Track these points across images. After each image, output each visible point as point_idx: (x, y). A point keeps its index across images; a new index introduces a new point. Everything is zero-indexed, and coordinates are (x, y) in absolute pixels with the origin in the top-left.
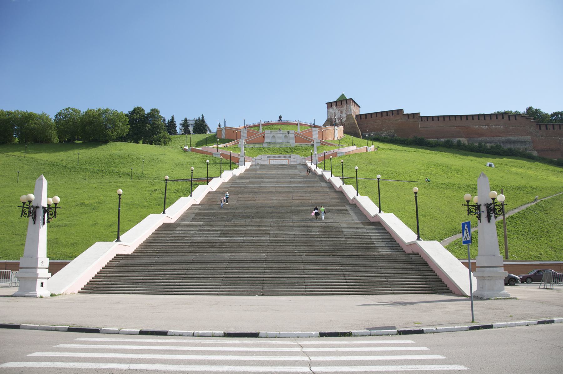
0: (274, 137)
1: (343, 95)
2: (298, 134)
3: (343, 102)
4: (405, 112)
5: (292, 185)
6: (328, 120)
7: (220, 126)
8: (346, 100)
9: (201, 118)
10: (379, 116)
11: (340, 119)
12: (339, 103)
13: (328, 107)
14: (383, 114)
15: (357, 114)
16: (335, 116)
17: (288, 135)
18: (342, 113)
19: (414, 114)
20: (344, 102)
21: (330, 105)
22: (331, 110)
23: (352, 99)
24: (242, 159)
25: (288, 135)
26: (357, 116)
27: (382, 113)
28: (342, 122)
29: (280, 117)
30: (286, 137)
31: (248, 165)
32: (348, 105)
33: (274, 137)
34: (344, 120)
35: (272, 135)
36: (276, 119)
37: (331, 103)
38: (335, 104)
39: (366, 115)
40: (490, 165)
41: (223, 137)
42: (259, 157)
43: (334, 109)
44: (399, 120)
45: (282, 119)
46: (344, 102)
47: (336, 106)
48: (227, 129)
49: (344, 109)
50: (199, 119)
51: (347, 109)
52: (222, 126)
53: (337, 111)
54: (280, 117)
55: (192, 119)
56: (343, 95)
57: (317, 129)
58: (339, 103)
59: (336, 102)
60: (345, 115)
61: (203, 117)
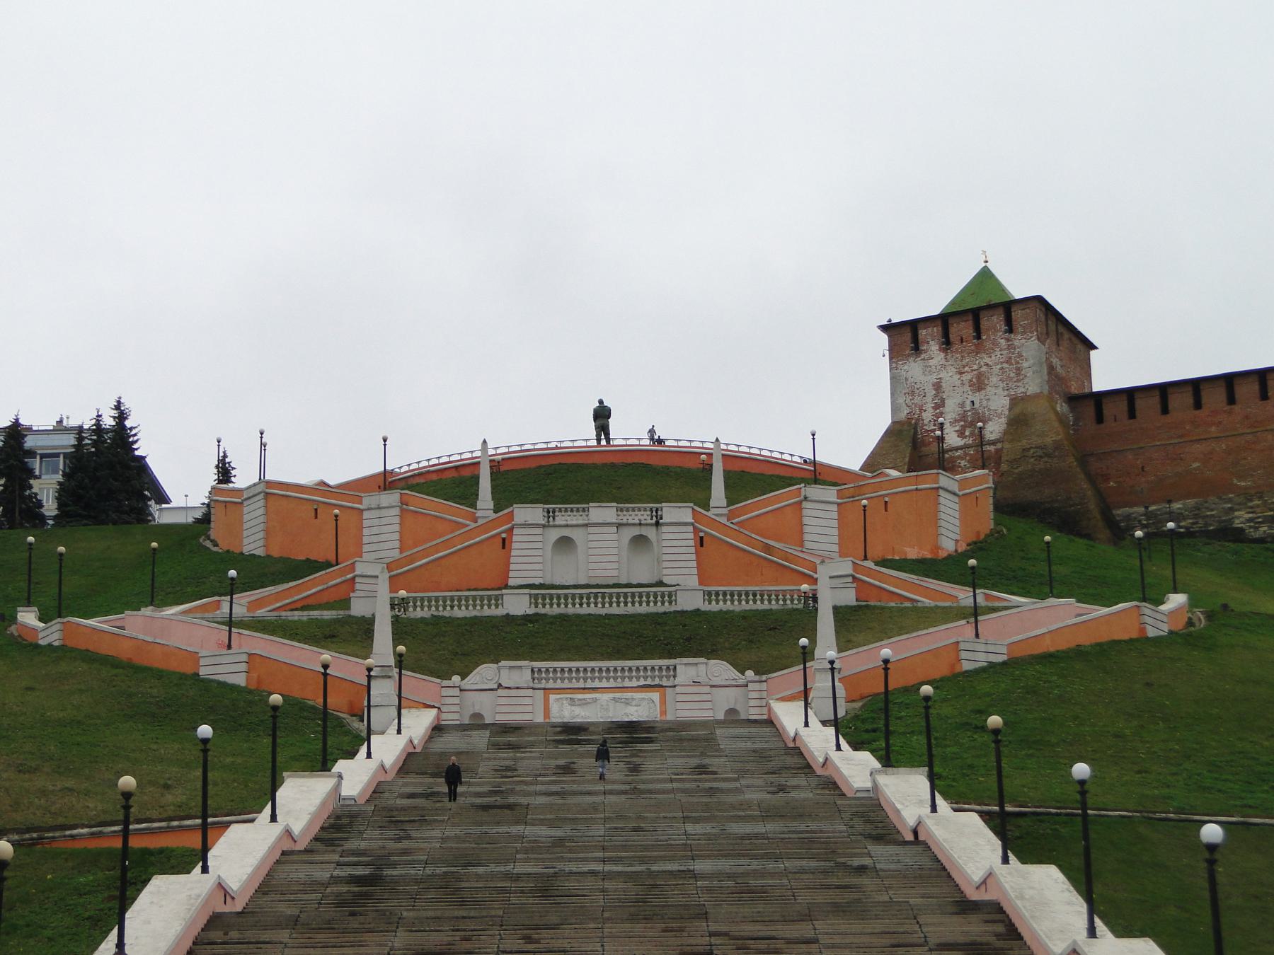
0: (565, 543)
1: (985, 276)
2: (713, 523)
3: (982, 315)
5: (699, 866)
6: (893, 434)
7: (224, 472)
8: (1008, 307)
9: (108, 422)
10: (1213, 399)
11: (972, 421)
12: (962, 329)
13: (895, 353)
14: (1242, 390)
15: (1074, 389)
16: (940, 405)
17: (651, 533)
18: (979, 384)
20: (995, 321)
21: (905, 336)
22: (913, 369)
23: (1039, 300)
24: (383, 691)
25: (651, 533)
26: (1073, 400)
27: (1229, 380)
28: (981, 441)
29: (602, 415)
30: (640, 541)
31: (418, 724)
32: (1017, 340)
33: (565, 543)
34: (994, 429)
35: (554, 534)
36: (582, 434)
37: (913, 326)
38: (936, 330)
39: (1130, 394)
41: (253, 543)
42: (485, 674)
43: (934, 364)
45: (612, 422)
46: (995, 321)
47: (947, 343)
48: (273, 493)
49: (993, 360)
50: (98, 429)
51: (1013, 359)
52: (244, 478)
53: (949, 377)
54: (602, 415)
55: (49, 424)
56: (985, 276)
57: (830, 494)
58: (962, 329)
59: (944, 320)
60: (997, 401)
61: (121, 416)
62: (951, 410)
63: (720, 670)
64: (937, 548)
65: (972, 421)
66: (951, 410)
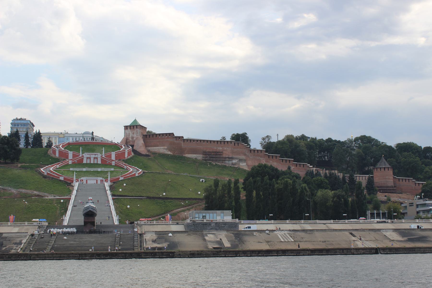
4: (176, 135)
12: (132, 127)
16: (129, 135)
18: (133, 134)
19: (179, 137)
21: (126, 127)
22: (127, 131)
26: (144, 135)
37: (127, 126)
40: (202, 181)
43: (129, 131)
44: (170, 140)
46: (136, 127)
49: (135, 131)
51: (137, 131)
53: (130, 133)
58: (132, 127)
59: (130, 126)
62: (130, 136)
63: (101, 178)
64: (125, 158)
65: (133, 138)
66: (130, 136)
